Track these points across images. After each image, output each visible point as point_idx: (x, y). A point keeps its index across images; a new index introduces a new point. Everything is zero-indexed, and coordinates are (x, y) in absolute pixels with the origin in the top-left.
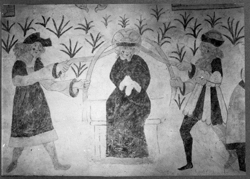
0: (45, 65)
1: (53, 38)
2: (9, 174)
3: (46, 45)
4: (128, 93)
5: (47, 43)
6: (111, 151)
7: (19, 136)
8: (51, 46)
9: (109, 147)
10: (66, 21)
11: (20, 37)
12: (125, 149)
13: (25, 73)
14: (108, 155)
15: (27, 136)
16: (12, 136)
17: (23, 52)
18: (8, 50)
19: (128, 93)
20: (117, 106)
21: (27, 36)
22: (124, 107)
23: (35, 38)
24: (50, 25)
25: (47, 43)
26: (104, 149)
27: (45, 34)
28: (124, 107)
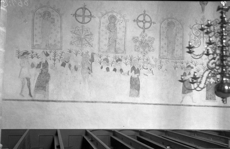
0: (191, 74)
1: (194, 66)
2: (181, 104)
3: (192, 68)
4: (212, 83)
5: (192, 68)
6: (207, 98)
7: (184, 93)
8: (193, 68)
9: (206, 97)
10: (197, 62)
11: (186, 66)
12: (210, 98)
13: (186, 76)
14: (206, 99)
15: (186, 93)
16: (182, 93)
17: (186, 70)
18: (182, 69)
19: (212, 83)
20: (209, 86)
21: (188, 65)
22: (211, 87)
23: (189, 66)
24: (193, 63)
25: (192, 68)
26: (205, 98)
27: (192, 65)
28: (211, 87)
